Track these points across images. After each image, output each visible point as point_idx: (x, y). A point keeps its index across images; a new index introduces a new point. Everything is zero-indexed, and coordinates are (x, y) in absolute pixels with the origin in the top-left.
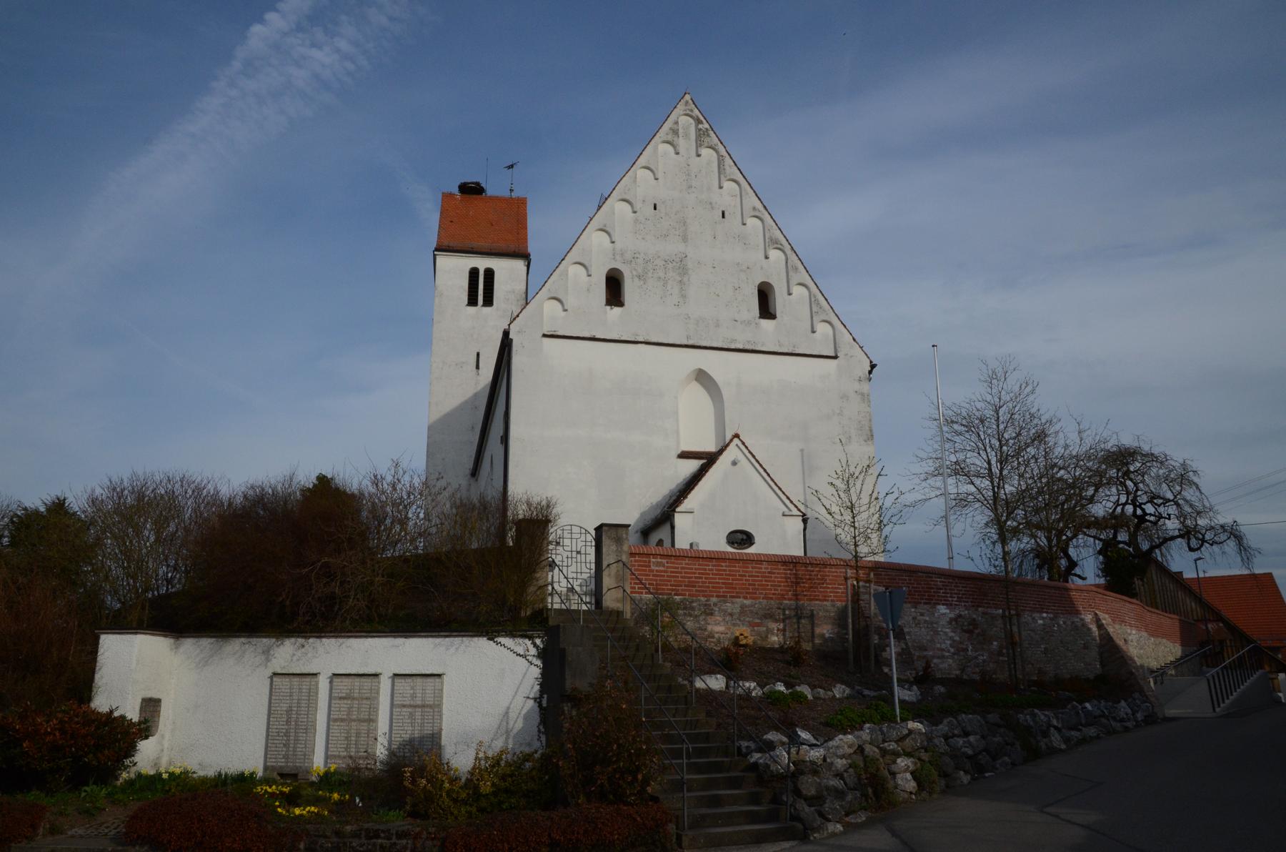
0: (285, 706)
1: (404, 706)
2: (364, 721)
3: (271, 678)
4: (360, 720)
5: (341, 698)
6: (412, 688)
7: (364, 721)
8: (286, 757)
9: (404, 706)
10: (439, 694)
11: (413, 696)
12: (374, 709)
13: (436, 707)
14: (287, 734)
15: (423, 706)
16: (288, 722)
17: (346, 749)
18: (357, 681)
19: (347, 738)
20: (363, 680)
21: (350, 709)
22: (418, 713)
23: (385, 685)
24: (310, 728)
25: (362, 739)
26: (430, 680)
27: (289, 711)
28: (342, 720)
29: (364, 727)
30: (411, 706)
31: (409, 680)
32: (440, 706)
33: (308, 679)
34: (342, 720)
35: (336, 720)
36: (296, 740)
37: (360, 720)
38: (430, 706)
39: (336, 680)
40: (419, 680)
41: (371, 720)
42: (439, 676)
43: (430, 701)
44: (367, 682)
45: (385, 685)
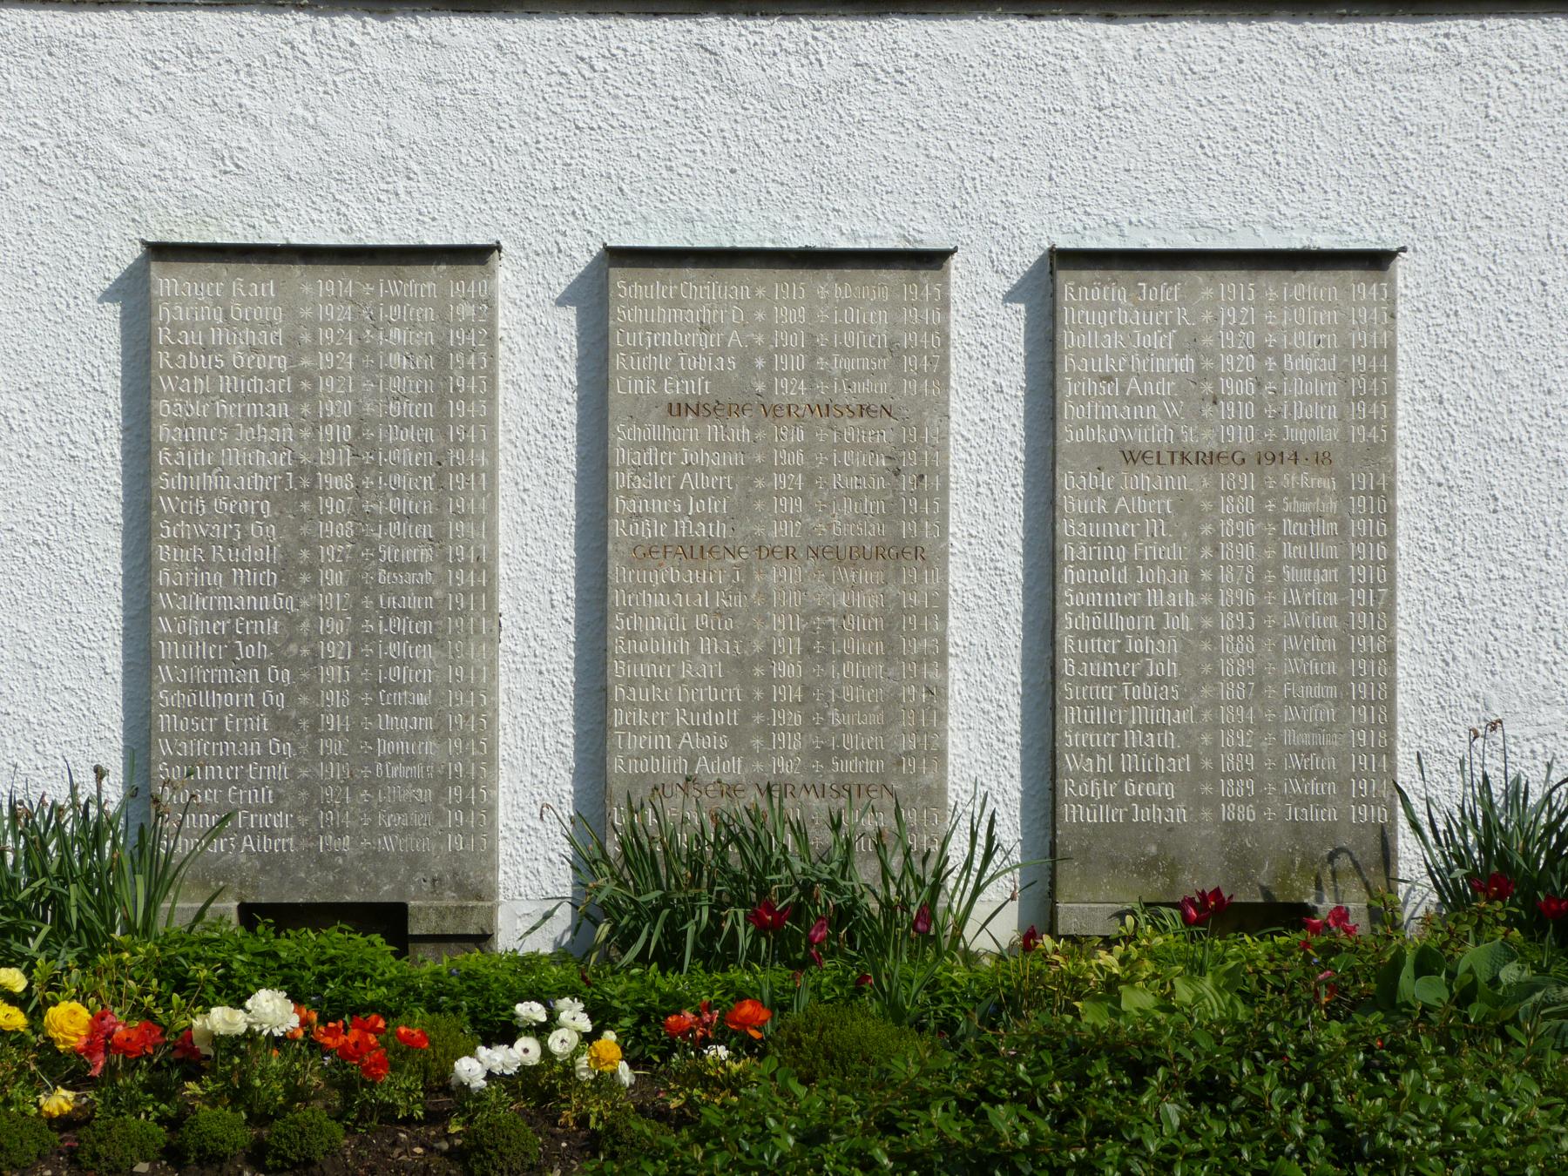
0: (263, 466)
1: (1133, 457)
2: (856, 555)
3: (132, 293)
4: (832, 555)
5: (677, 409)
6: (1189, 342)
7: (856, 555)
8: (306, 797)
9: (1133, 457)
10: (1371, 382)
11: (1200, 392)
12: (916, 480)
14: (295, 651)
15: (1270, 457)
16: (293, 570)
19: (739, 667)
20: (828, 285)
22: (1235, 504)
24: (459, 607)
27: (299, 490)
28: (694, 552)
29: (861, 593)
30: (1183, 457)
32: (1380, 453)
33: (427, 282)
34: (694, 552)
35: (646, 553)
36: (372, 687)
37: (832, 555)
38: (1321, 459)
39: (626, 285)
41: (906, 549)
42: (1376, 261)
43: (1313, 419)
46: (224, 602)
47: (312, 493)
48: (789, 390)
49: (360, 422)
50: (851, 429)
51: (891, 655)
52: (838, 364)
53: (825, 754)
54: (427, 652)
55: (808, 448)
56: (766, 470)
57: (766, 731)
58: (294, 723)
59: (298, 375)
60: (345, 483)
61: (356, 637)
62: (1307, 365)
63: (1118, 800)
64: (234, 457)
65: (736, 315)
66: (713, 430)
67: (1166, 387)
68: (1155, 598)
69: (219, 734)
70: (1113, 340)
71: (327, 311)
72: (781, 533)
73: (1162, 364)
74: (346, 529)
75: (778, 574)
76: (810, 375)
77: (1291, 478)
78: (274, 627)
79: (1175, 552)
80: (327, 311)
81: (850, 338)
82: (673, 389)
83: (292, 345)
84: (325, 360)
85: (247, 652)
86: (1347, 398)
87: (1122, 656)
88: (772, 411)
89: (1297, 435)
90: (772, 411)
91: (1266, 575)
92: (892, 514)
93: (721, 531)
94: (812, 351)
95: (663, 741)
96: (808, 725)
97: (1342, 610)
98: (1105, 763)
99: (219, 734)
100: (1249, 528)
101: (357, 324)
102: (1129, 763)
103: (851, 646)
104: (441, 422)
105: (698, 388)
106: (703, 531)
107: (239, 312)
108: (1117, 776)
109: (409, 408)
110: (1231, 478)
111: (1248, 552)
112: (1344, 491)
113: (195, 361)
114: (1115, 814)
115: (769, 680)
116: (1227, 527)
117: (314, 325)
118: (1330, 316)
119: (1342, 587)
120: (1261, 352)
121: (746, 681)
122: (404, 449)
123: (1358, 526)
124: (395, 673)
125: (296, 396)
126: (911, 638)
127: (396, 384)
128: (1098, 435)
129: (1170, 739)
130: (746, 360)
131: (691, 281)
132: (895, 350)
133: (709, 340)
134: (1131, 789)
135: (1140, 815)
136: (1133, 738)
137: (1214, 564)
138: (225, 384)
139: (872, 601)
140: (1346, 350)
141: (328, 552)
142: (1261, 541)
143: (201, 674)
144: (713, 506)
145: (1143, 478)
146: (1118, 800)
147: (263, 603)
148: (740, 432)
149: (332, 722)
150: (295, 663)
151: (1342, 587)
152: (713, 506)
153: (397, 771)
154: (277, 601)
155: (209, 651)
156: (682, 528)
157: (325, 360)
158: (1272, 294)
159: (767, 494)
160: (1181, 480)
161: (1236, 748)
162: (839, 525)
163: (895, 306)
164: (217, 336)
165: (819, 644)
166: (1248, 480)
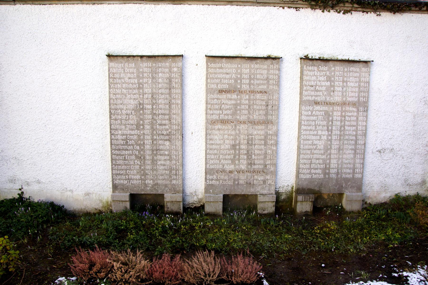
1: (317, 103)
2: (259, 123)
4: (253, 123)
5: (221, 91)
6: (329, 79)
7: (259, 123)
9: (317, 103)
10: (365, 89)
13: (362, 105)
15: (344, 104)
17: (233, 161)
18: (246, 68)
19: (234, 147)
20: (254, 65)
21: (236, 107)
23: (291, 71)
25: (257, 149)
26: (354, 68)
27: (140, 108)
28: (223, 122)
31: (324, 68)
33: (167, 63)
34: (223, 122)
36: (156, 151)
37: (253, 123)
40: (338, 68)
44: (262, 69)
45: (291, 71)
46: (125, 132)
47: (143, 109)
48: (245, 87)
49: (153, 94)
50: (258, 96)
51: (266, 144)
52: (256, 82)
53: (251, 164)
54: (167, 143)
55: (249, 100)
56: (240, 104)
57: (239, 160)
58: (141, 158)
59: (139, 84)
60: (150, 107)
61: (153, 140)
62: (352, 84)
63: (310, 173)
64: (126, 101)
65: (234, 71)
66: (229, 96)
67: (324, 88)
68: (320, 132)
69: (125, 159)
70: (314, 78)
71: (146, 70)
72: (243, 118)
73: (323, 84)
74: (150, 117)
75: (242, 126)
76: (250, 84)
77: (347, 108)
78: (136, 137)
79: (325, 123)
80: (146, 70)
81: (258, 76)
82: (220, 87)
83: (138, 77)
84: (145, 80)
85: (130, 142)
86: (360, 92)
87: (313, 144)
88: (241, 92)
89: (349, 99)
90: (241, 92)
91: (342, 128)
92: (266, 114)
93: (230, 117)
94: (250, 79)
95: (217, 161)
96: (248, 158)
97: (356, 136)
98: (308, 166)
99: (125, 159)
100: (339, 118)
101: (152, 72)
102: (313, 166)
103: (257, 142)
104: (170, 94)
105: (226, 87)
106: (226, 117)
107: (127, 70)
108: (310, 169)
109: (163, 91)
110: (336, 108)
111: (338, 123)
112: (358, 111)
113: (118, 81)
114: (308, 176)
115: (240, 149)
116: (335, 118)
117: (143, 73)
118: (358, 74)
119: (356, 131)
120: (343, 81)
121: (235, 149)
122: (162, 101)
123: (360, 118)
124: (161, 147)
125: (139, 88)
126: (272, 141)
127: (160, 86)
128: (310, 98)
129: (321, 161)
130: (236, 81)
131: (224, 63)
132: (267, 79)
133: (228, 76)
134: (313, 171)
135: (314, 176)
136: (314, 161)
137: (332, 126)
138: (124, 86)
139: (262, 132)
140: (360, 81)
141: (146, 121)
142: (341, 121)
143: (121, 147)
144: (228, 112)
145: (318, 108)
146: (310, 173)
147: (133, 132)
148: (234, 96)
149: (148, 157)
150: (140, 145)
151: (356, 131)
152: (228, 112)
153: (162, 167)
154: (135, 132)
155: (122, 142)
156: (222, 117)
157: (145, 80)
158: (346, 69)
159: (240, 110)
160: (326, 108)
161: (334, 163)
162: (255, 117)
163: (268, 70)
164: (122, 75)
165: (250, 142)
166: (339, 108)
